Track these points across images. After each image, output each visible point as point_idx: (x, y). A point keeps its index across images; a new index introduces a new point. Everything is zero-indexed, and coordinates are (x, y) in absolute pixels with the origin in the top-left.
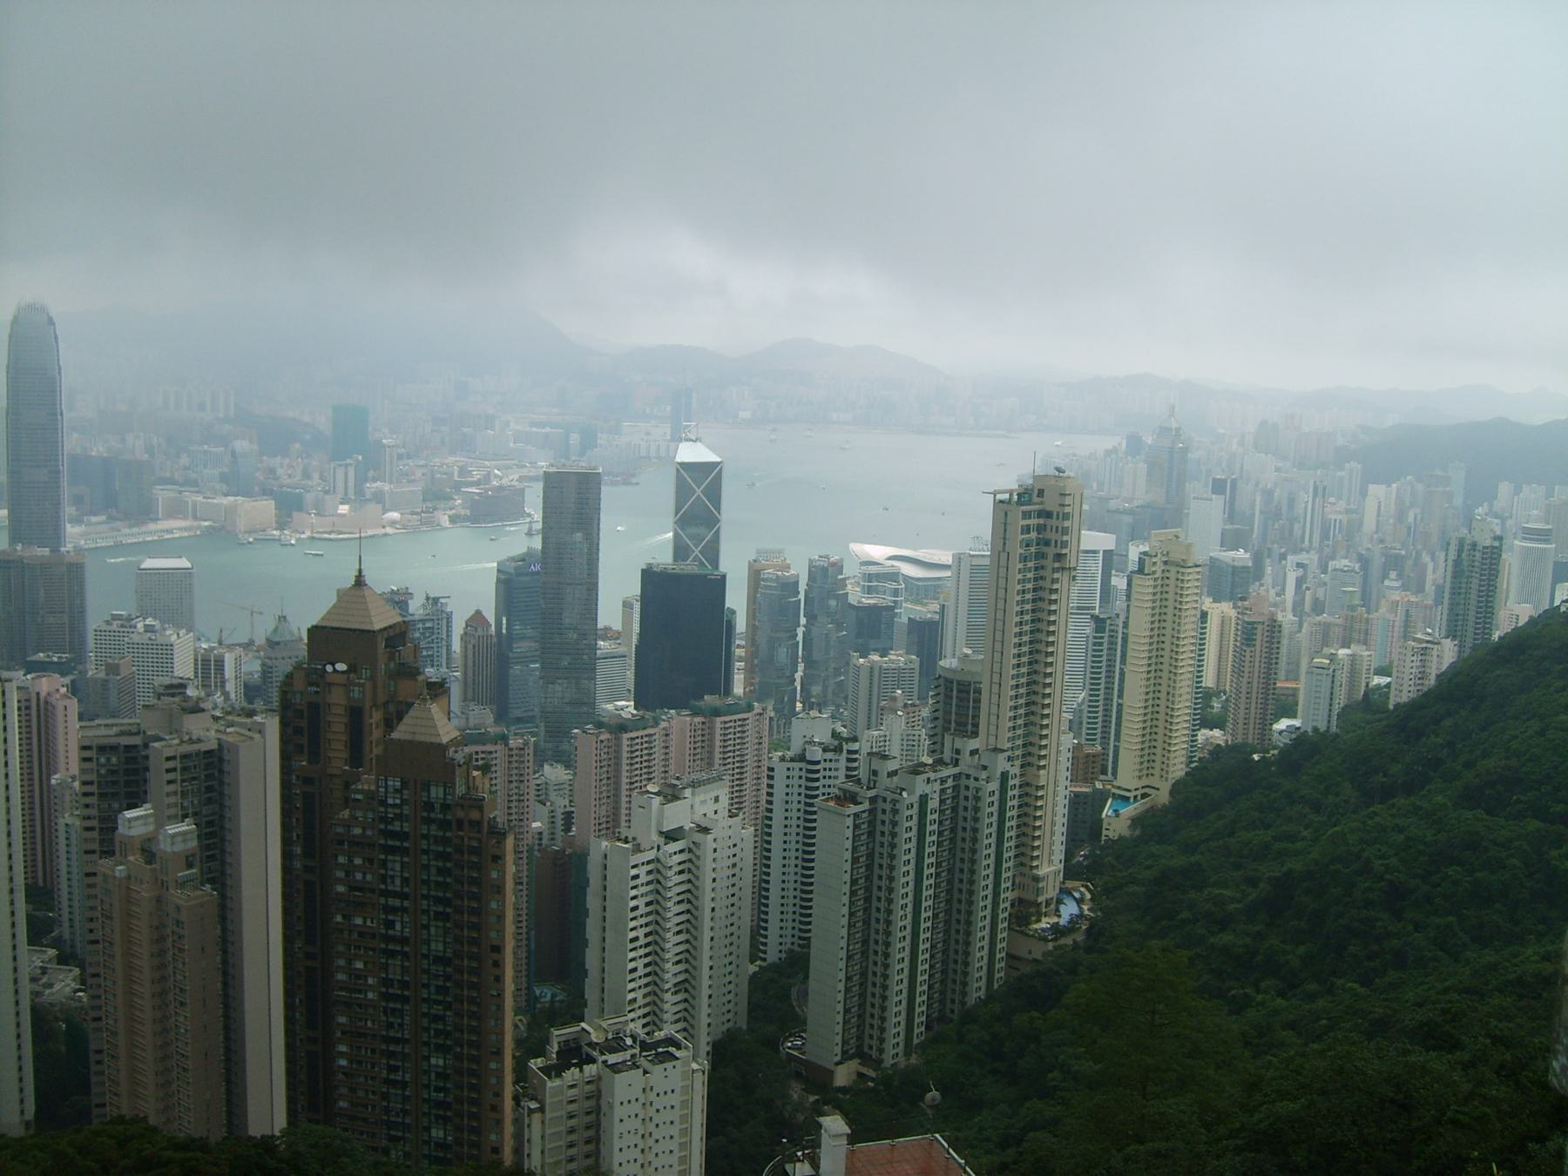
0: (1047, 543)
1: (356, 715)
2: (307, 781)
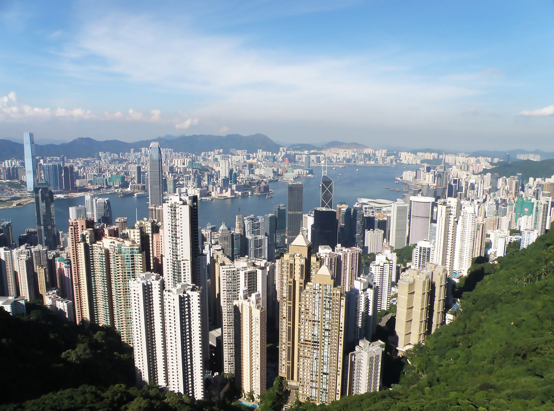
0: (451, 214)
1: (302, 266)
2: (290, 282)
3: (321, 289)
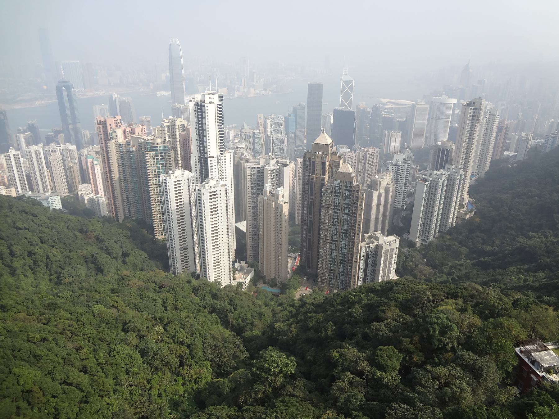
3: (341, 186)
